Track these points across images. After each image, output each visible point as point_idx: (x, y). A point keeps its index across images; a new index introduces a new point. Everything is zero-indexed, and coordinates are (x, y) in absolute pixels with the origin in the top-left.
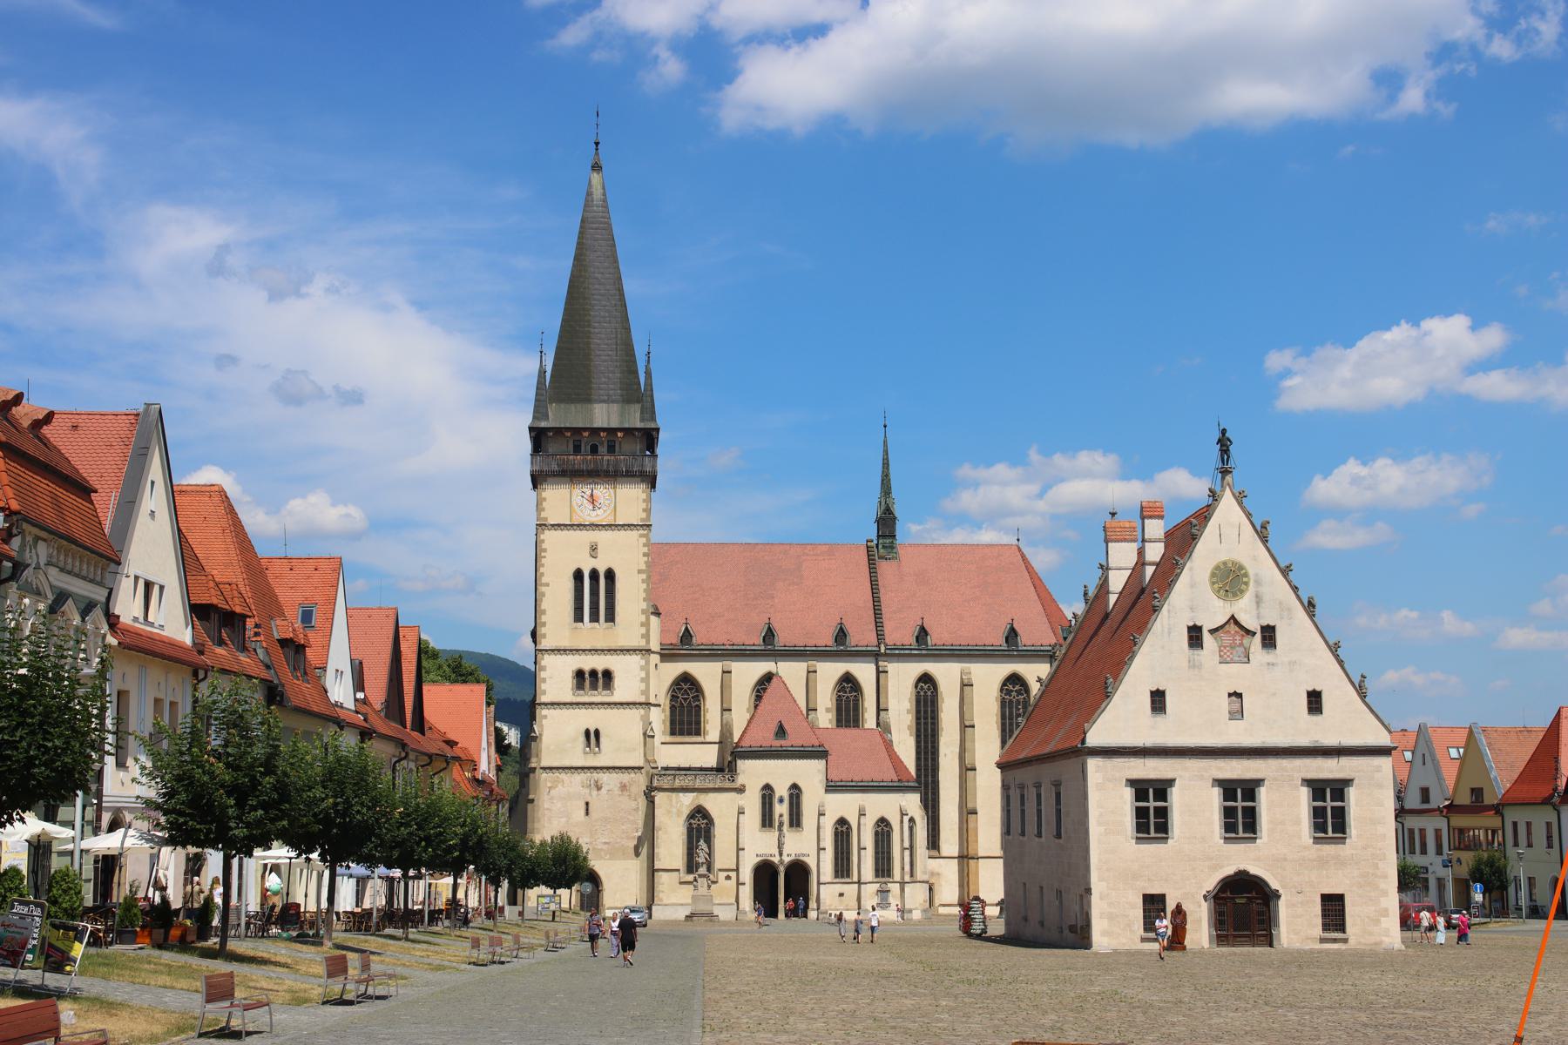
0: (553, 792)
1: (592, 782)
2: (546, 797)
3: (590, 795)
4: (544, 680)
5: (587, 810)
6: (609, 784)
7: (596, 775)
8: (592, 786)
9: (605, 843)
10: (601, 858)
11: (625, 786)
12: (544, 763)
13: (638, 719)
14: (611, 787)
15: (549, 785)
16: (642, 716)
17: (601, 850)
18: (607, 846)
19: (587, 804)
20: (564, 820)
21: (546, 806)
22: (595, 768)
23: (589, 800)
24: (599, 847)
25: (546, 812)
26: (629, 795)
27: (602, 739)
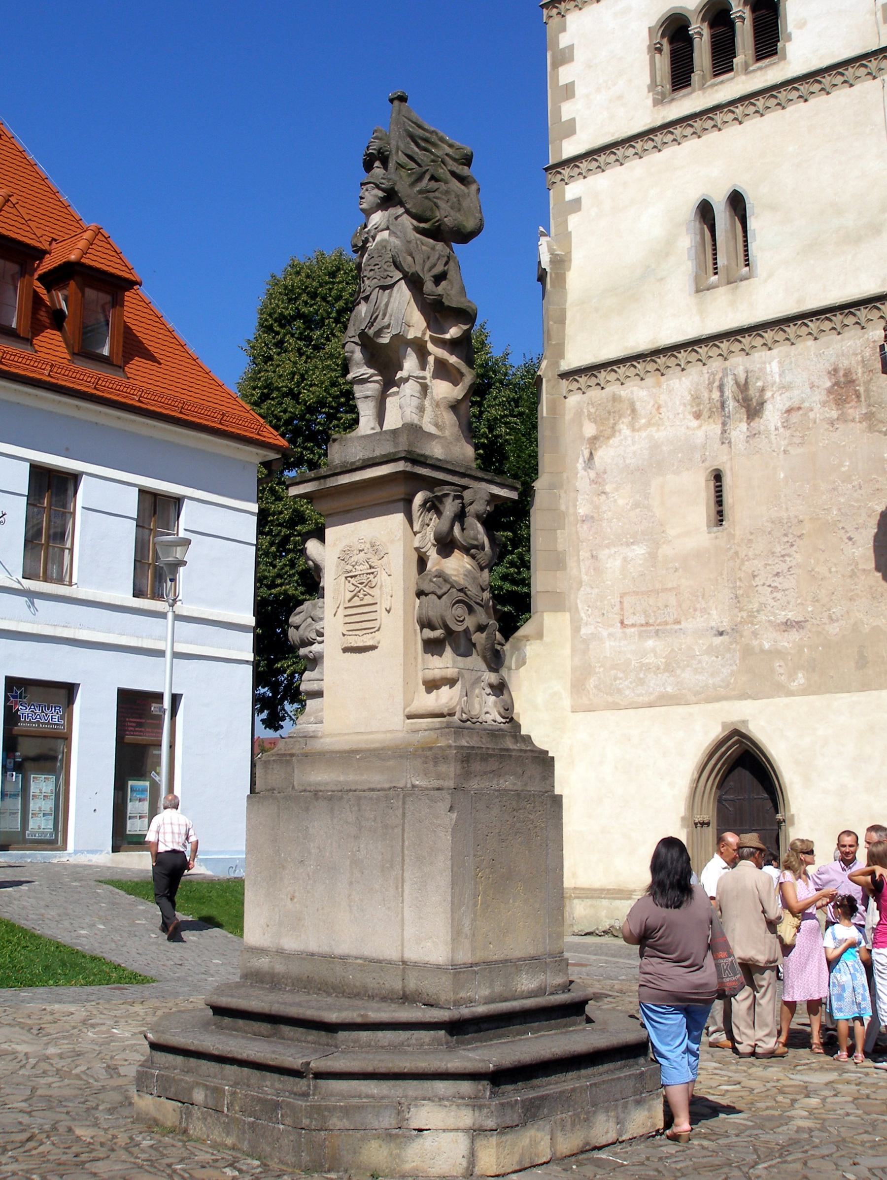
0: (599, 455)
1: (728, 393)
2: (582, 478)
3: (725, 439)
4: (569, 91)
5: (719, 502)
6: (785, 388)
7: (739, 364)
8: (731, 404)
9: (788, 625)
10: (781, 690)
11: (852, 382)
12: (573, 359)
14: (795, 396)
15: (590, 430)
17: (777, 653)
18: (794, 635)
19: (718, 477)
20: (640, 550)
21: (582, 511)
23: (722, 460)
24: (767, 646)
25: (584, 530)
26: (869, 417)
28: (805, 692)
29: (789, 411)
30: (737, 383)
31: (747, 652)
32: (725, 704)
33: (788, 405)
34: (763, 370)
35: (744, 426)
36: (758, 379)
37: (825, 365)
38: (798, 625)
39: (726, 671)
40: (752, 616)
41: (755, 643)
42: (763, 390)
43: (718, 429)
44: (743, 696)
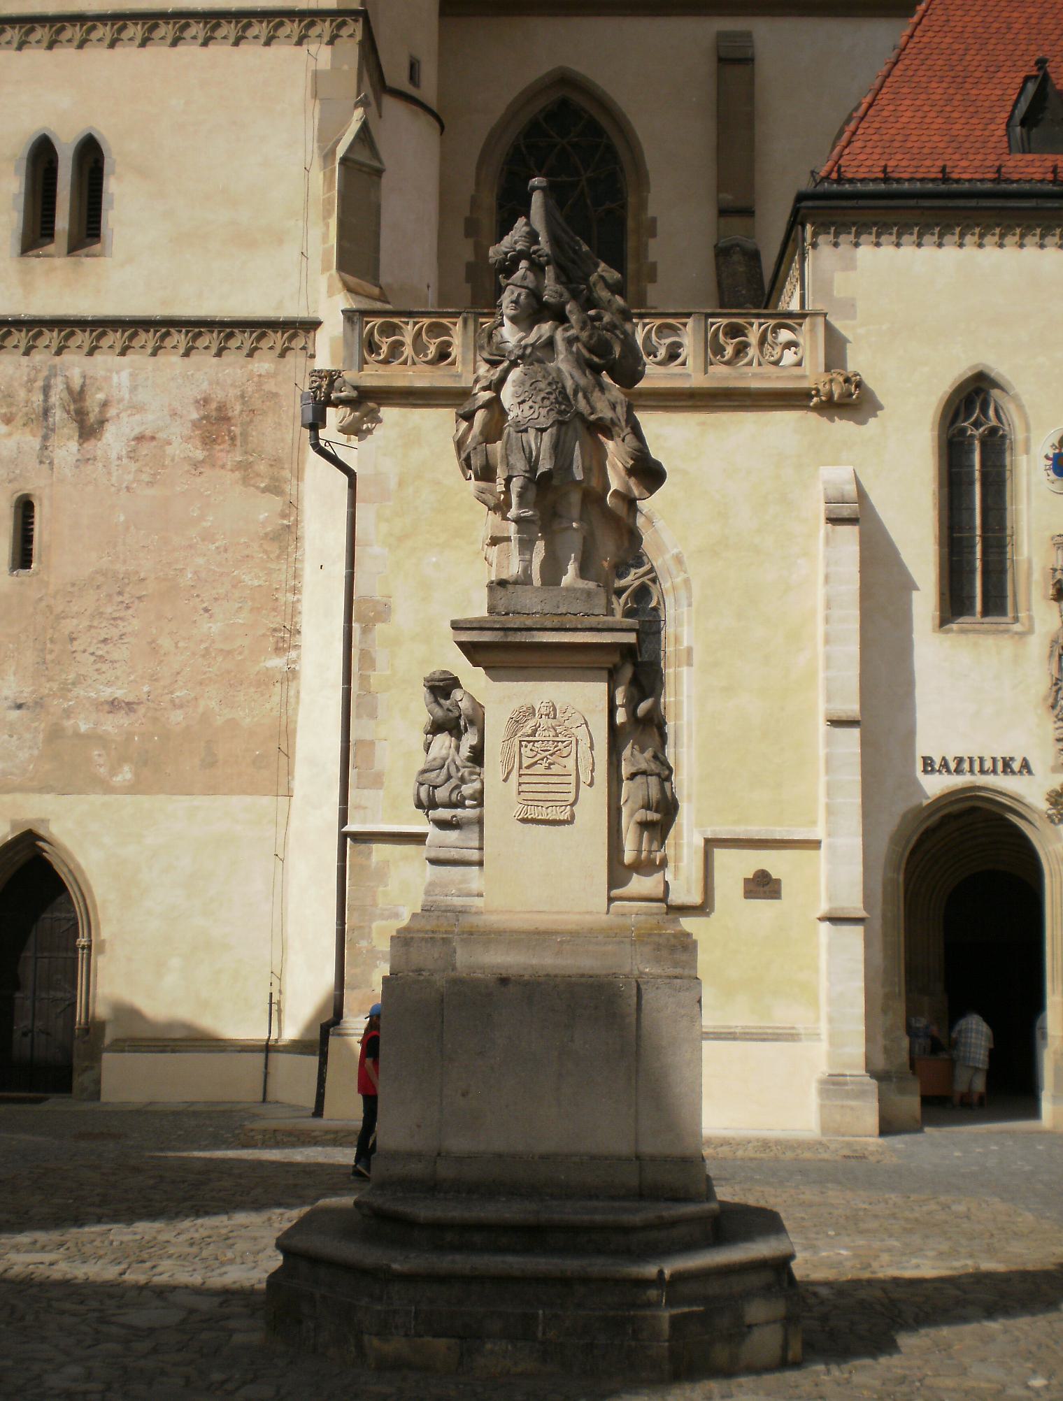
1: (54, 399)
3: (44, 456)
6: (137, 408)
7: (75, 366)
8: (58, 415)
9: (114, 705)
11: (227, 419)
13: (299, 90)
14: (149, 421)
16: (316, 75)
17: (100, 740)
22: (67, 326)
23: (36, 484)
24: (83, 728)
26: (244, 466)
27: (112, 186)
28: (133, 789)
29: (140, 438)
30: (69, 389)
31: (55, 734)
32: (19, 797)
33: (137, 431)
34: (107, 379)
35: (73, 445)
36: (99, 389)
37: (194, 392)
38: (130, 707)
39: (23, 755)
40: (65, 689)
41: (68, 724)
42: (105, 405)
43: (36, 443)
44: (44, 789)
